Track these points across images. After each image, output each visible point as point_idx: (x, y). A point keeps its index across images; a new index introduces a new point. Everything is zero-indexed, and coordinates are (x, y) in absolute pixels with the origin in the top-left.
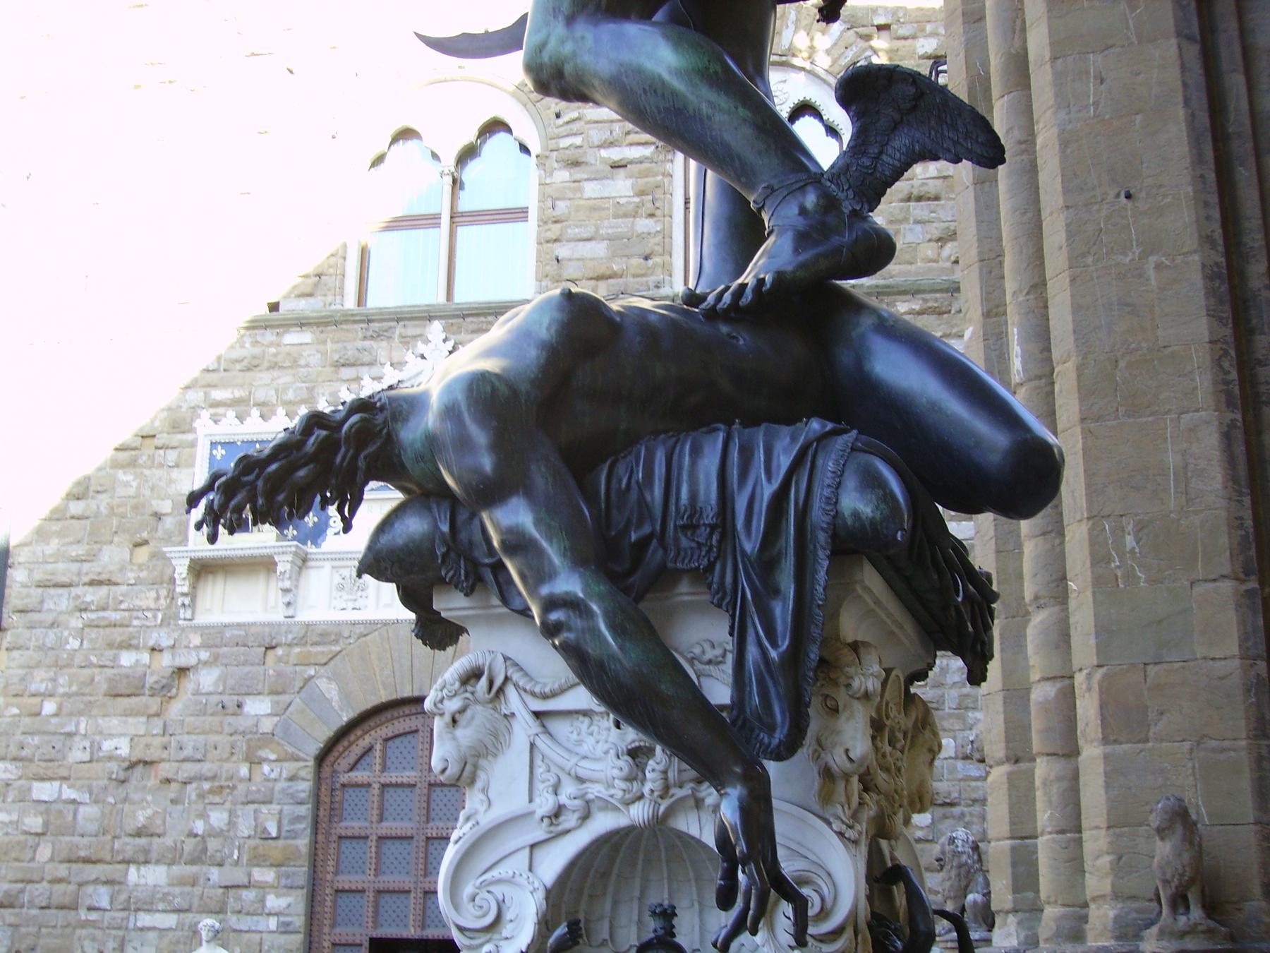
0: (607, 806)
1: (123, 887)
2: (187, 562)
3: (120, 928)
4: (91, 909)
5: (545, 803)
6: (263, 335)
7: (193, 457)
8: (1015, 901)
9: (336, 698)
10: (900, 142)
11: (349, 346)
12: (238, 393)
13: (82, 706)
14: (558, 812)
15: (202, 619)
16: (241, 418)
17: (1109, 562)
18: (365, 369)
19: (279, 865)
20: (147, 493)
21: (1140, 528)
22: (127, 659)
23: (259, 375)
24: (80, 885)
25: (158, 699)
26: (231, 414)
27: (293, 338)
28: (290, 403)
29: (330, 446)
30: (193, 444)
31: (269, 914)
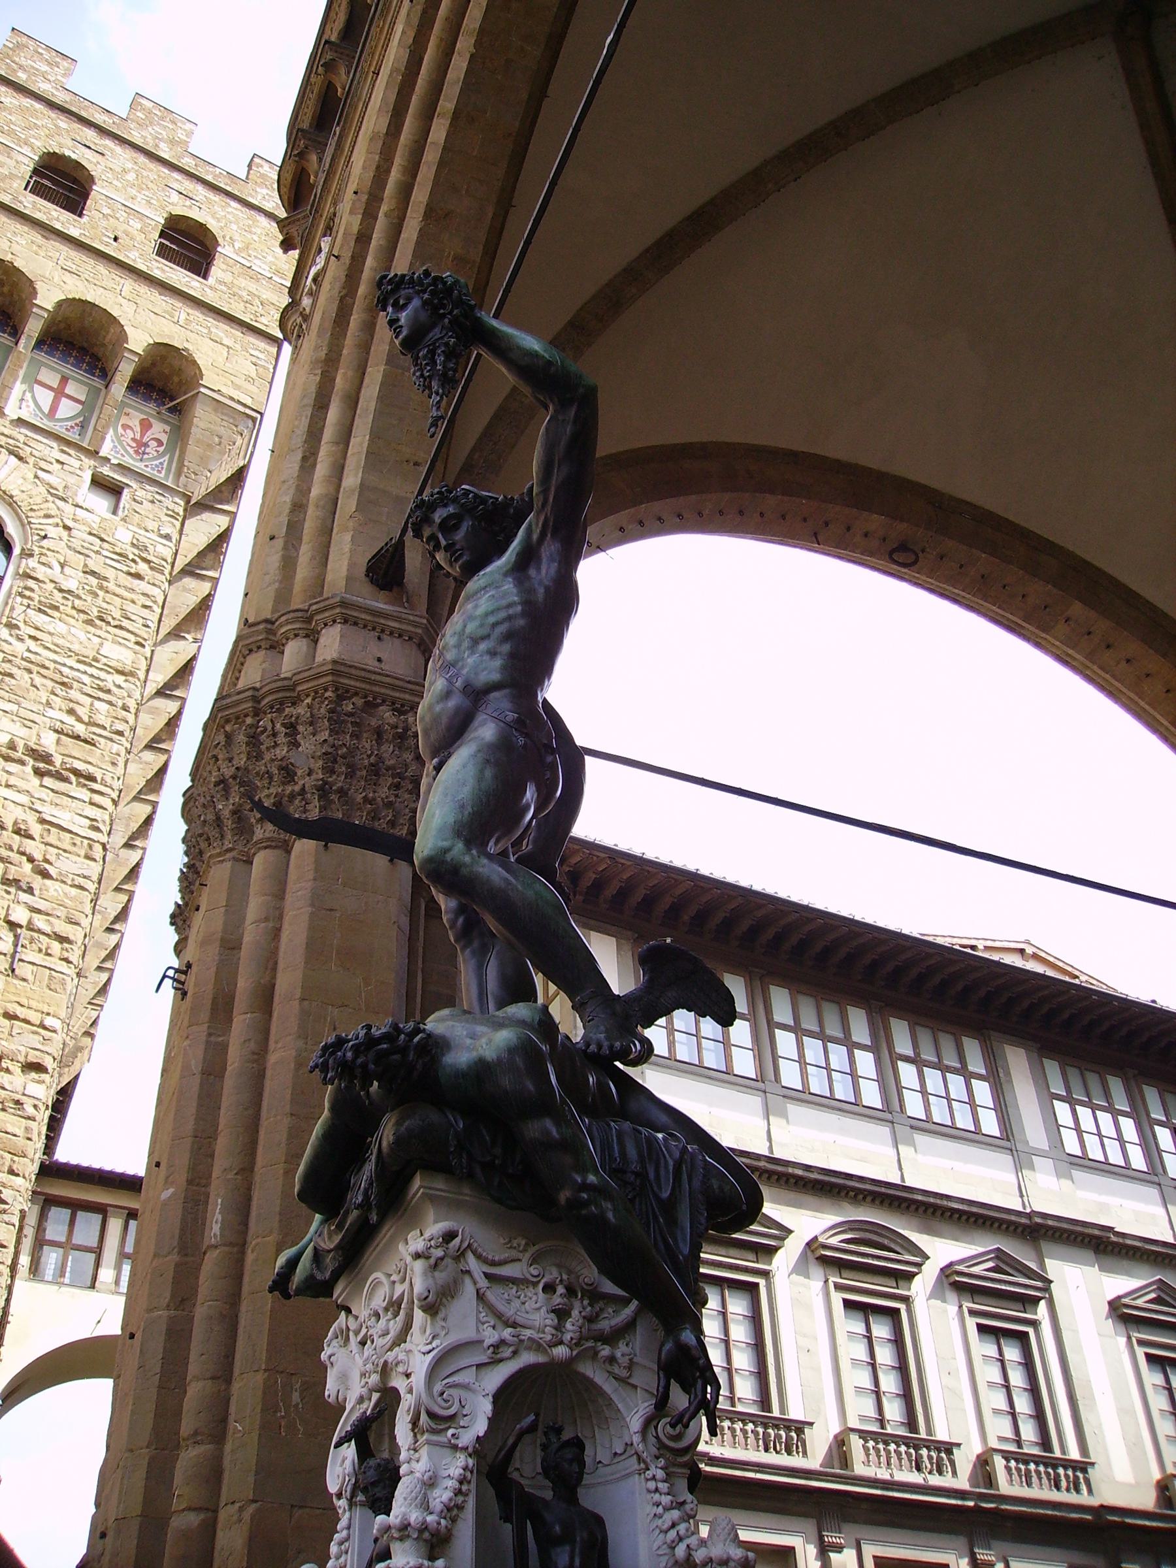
17: (276, 1412)
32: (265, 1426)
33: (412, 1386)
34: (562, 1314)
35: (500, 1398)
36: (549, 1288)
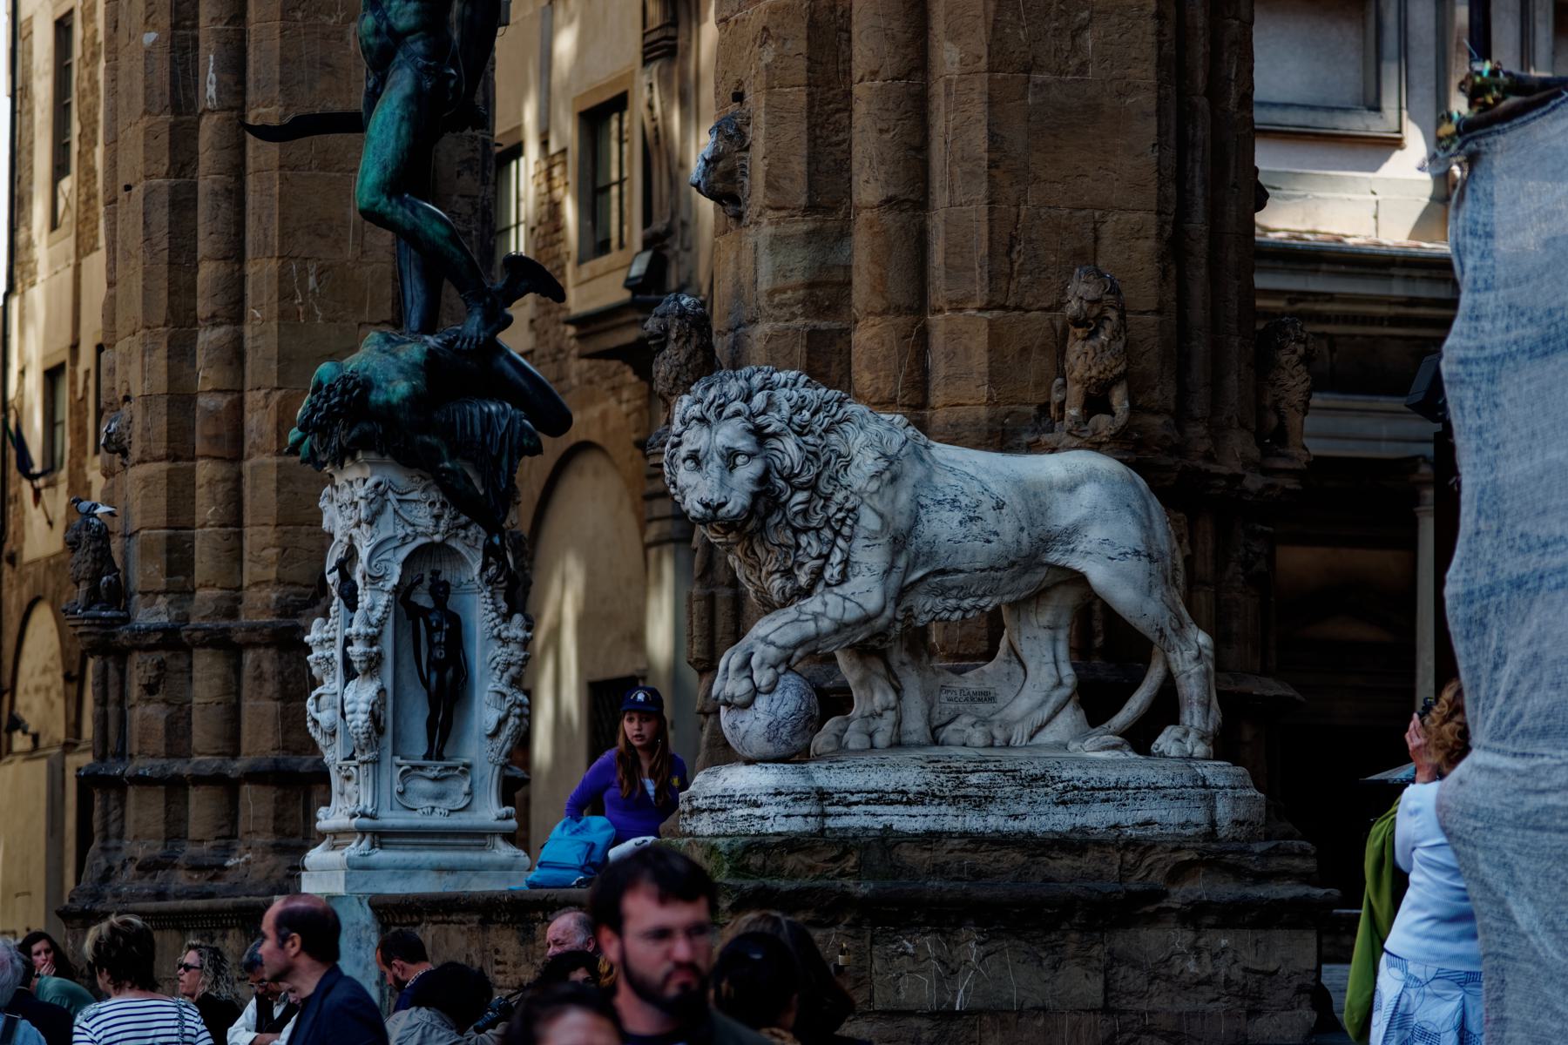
0: (424, 534)
8: (168, 583)
10: (524, 284)
21: (321, 272)
32: (282, 315)
33: (364, 554)
34: (438, 518)
35: (406, 564)
36: (432, 504)
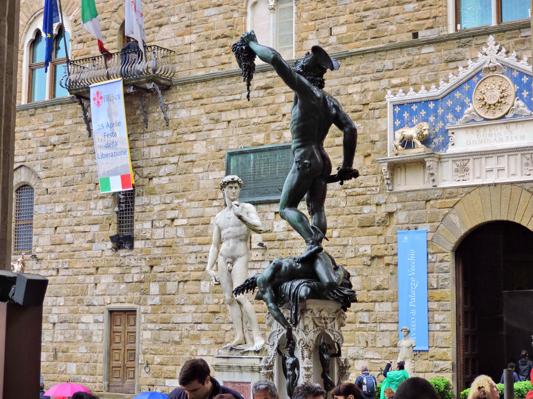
1: (374, 313)
2: (387, 164)
3: (373, 331)
4: (361, 323)
5: (278, 329)
6: (412, 50)
7: (386, 112)
9: (458, 223)
11: (452, 51)
12: (404, 80)
13: (349, 232)
14: (280, 330)
15: (397, 189)
16: (405, 92)
18: (460, 62)
19: (439, 301)
20: (368, 131)
22: (366, 209)
23: (412, 70)
24: (356, 312)
25: (381, 227)
26: (401, 90)
27: (426, 50)
28: (427, 82)
29: (248, 284)
30: (386, 107)
31: (436, 323)
